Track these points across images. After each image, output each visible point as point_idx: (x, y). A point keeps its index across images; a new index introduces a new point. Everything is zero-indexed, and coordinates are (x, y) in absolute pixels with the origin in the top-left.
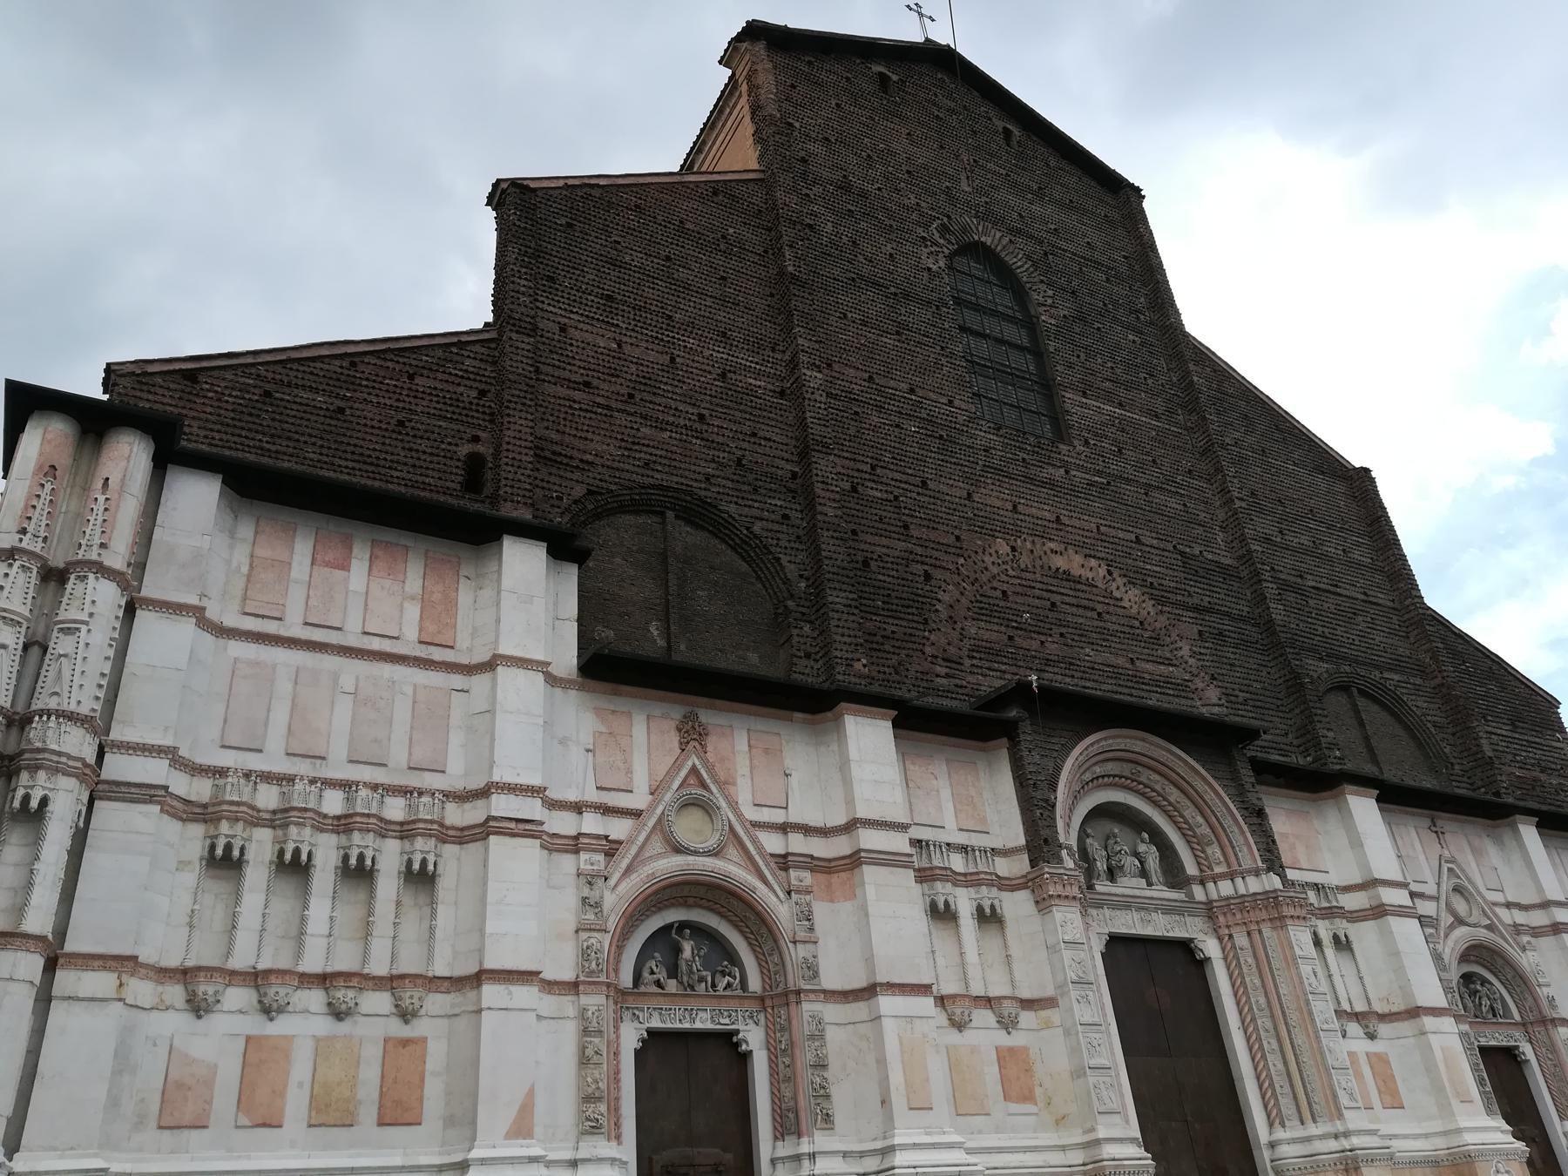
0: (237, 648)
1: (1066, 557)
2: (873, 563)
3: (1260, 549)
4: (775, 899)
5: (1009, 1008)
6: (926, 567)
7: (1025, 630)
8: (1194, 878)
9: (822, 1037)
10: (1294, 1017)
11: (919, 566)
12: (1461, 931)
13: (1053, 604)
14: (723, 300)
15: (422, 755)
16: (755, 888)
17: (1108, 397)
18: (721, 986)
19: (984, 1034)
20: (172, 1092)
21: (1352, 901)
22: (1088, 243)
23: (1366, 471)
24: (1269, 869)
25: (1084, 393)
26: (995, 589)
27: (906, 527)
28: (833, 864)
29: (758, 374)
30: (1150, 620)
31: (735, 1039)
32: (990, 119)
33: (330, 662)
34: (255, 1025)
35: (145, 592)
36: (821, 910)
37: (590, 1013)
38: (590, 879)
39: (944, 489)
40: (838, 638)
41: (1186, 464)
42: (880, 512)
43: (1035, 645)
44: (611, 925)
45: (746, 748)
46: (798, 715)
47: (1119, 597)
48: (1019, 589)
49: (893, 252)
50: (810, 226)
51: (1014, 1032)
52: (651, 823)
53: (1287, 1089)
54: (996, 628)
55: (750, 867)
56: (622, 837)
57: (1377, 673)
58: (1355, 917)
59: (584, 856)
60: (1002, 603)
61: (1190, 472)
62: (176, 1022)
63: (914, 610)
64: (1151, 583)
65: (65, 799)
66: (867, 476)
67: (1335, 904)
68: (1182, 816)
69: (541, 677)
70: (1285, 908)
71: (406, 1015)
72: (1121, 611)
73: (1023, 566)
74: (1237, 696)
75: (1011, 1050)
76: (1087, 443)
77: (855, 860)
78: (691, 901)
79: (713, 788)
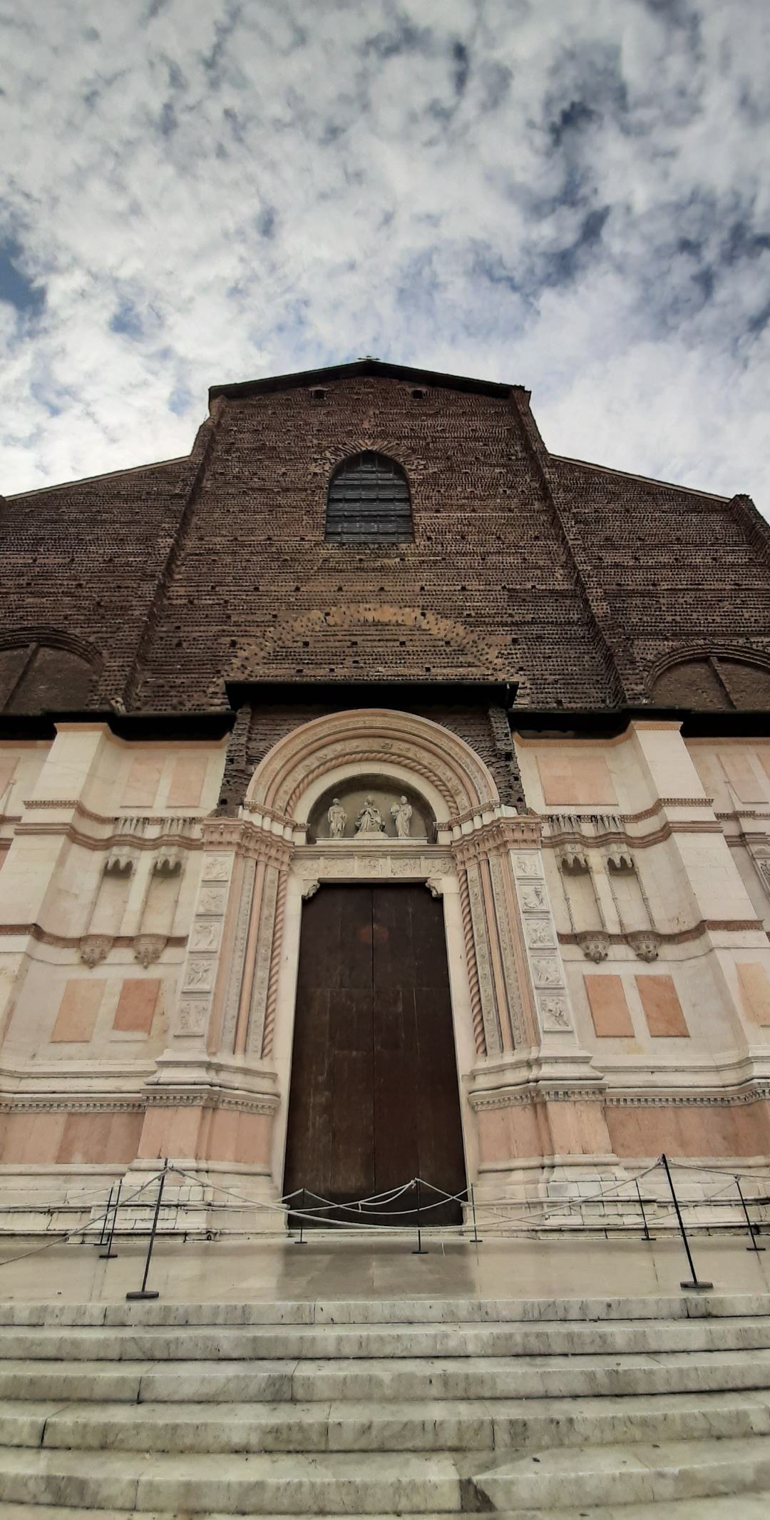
1: (379, 611)
2: (185, 645)
5: (145, 946)
6: (233, 638)
7: (316, 664)
8: (441, 826)
10: (505, 938)
11: (228, 639)
13: (355, 644)
17: (462, 508)
23: (743, 498)
26: (297, 642)
27: (229, 617)
30: (459, 639)
39: (273, 588)
40: (104, 688)
42: (205, 612)
47: (428, 628)
48: (324, 638)
49: (283, 470)
50: (222, 474)
51: (152, 967)
53: (493, 1015)
54: (287, 666)
57: (741, 641)
58: (646, 842)
60: (302, 650)
61: (537, 538)
63: (209, 666)
64: (469, 616)
66: (203, 593)
67: (614, 831)
68: (436, 775)
70: (508, 836)
73: (332, 623)
74: (546, 679)
75: (139, 984)
76: (429, 539)
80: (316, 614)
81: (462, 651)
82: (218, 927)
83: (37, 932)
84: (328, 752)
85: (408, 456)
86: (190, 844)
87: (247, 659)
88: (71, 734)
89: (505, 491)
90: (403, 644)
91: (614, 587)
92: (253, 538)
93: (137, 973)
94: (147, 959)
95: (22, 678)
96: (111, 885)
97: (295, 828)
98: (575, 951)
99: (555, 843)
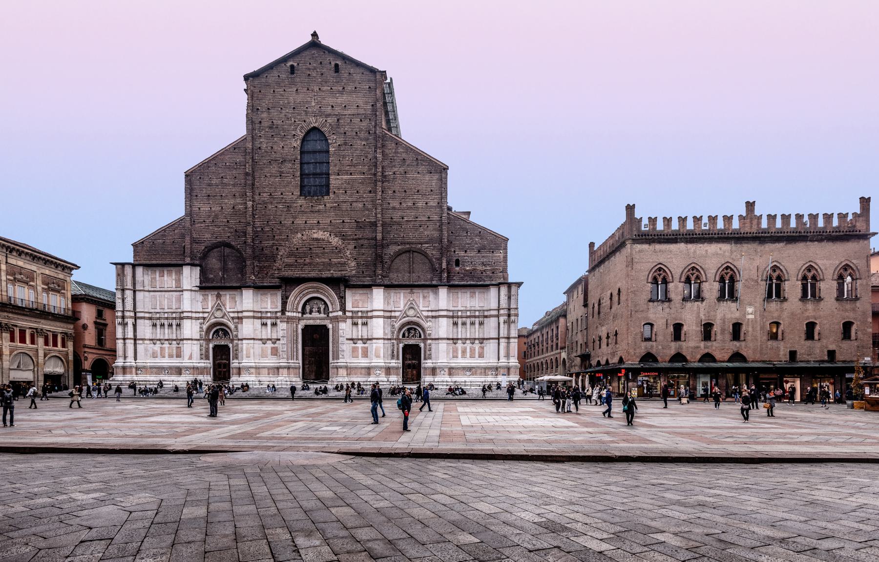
0: (152, 293)
3: (380, 216)
5: (273, 340)
12: (407, 318)
13: (311, 248)
14: (234, 185)
15: (177, 307)
19: (269, 345)
20: (153, 353)
21: (370, 314)
22: (358, 106)
24: (340, 310)
25: (338, 174)
27: (274, 237)
29: (242, 204)
32: (330, 63)
33: (164, 293)
34: (160, 345)
35: (137, 289)
36: (239, 326)
38: (201, 324)
41: (369, 189)
43: (302, 261)
50: (260, 148)
57: (420, 246)
61: (370, 192)
62: (152, 345)
64: (343, 235)
65: (130, 322)
71: (178, 344)
72: (330, 246)
76: (334, 192)
77: (240, 319)
80: (299, 235)
81: (340, 252)
82: (285, 339)
83: (254, 339)
84: (304, 292)
85: (329, 132)
86: (277, 318)
87: (282, 256)
89: (364, 159)
90: (324, 248)
91: (390, 220)
92: (276, 194)
93: (273, 345)
94: (274, 343)
95: (224, 261)
96: (263, 327)
97: (299, 312)
98: (351, 342)
99: (352, 318)
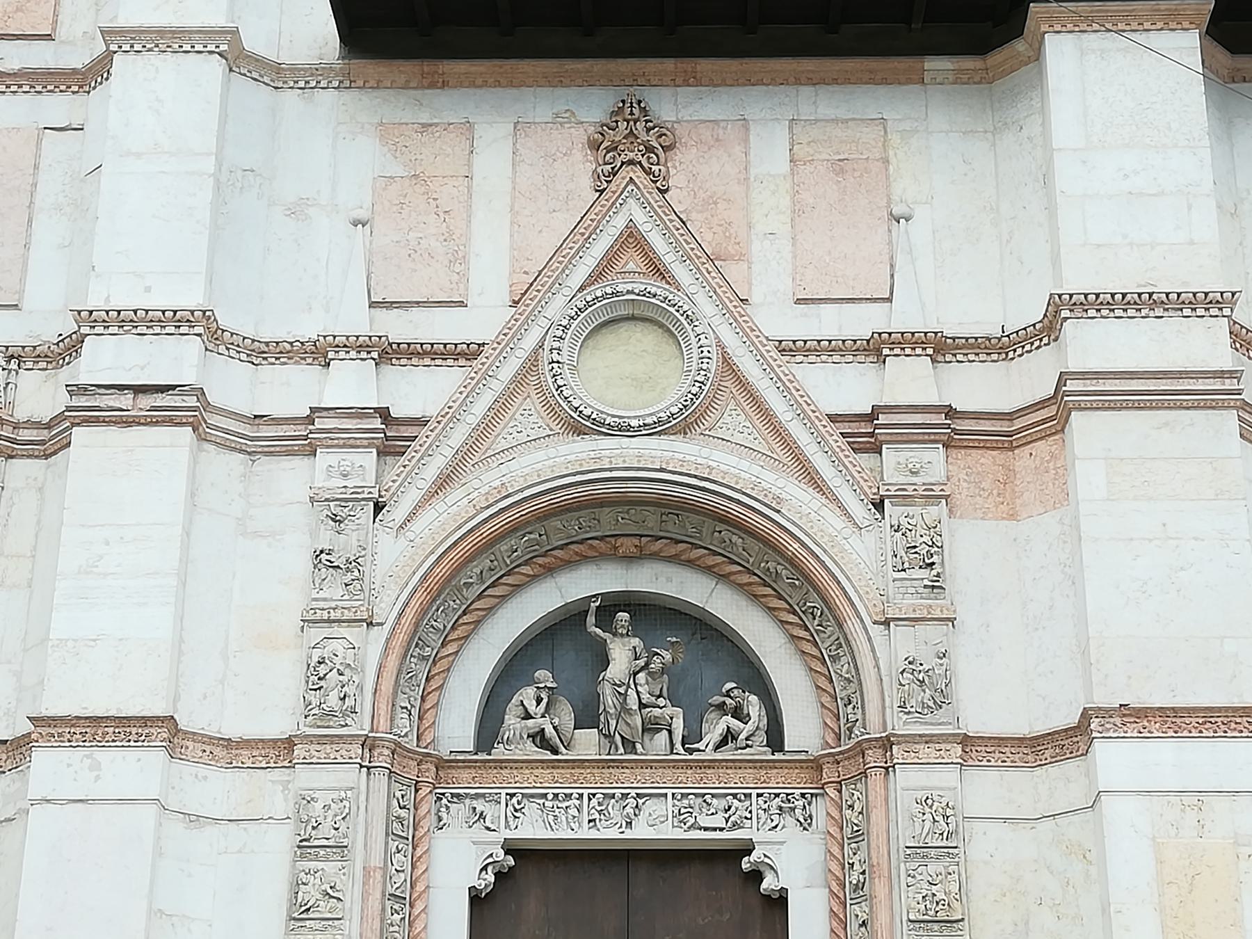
4: (834, 521)
9: (948, 852)
16: (779, 499)
18: (713, 734)
28: (1018, 424)
31: (745, 865)
37: (319, 806)
44: (386, 610)
45: (782, 164)
46: (936, 65)
52: (507, 372)
55: (780, 453)
56: (431, 411)
59: (325, 458)
69: (216, 66)
78: (628, 545)
79: (681, 273)
88: (1095, 41)
